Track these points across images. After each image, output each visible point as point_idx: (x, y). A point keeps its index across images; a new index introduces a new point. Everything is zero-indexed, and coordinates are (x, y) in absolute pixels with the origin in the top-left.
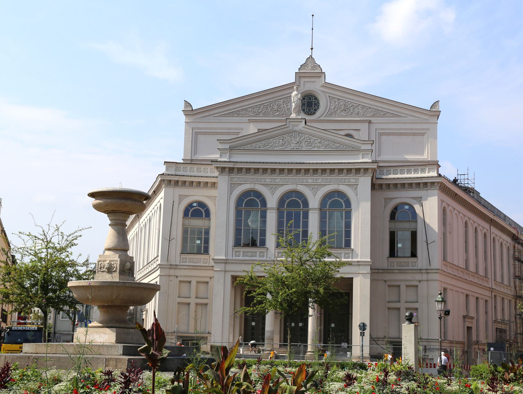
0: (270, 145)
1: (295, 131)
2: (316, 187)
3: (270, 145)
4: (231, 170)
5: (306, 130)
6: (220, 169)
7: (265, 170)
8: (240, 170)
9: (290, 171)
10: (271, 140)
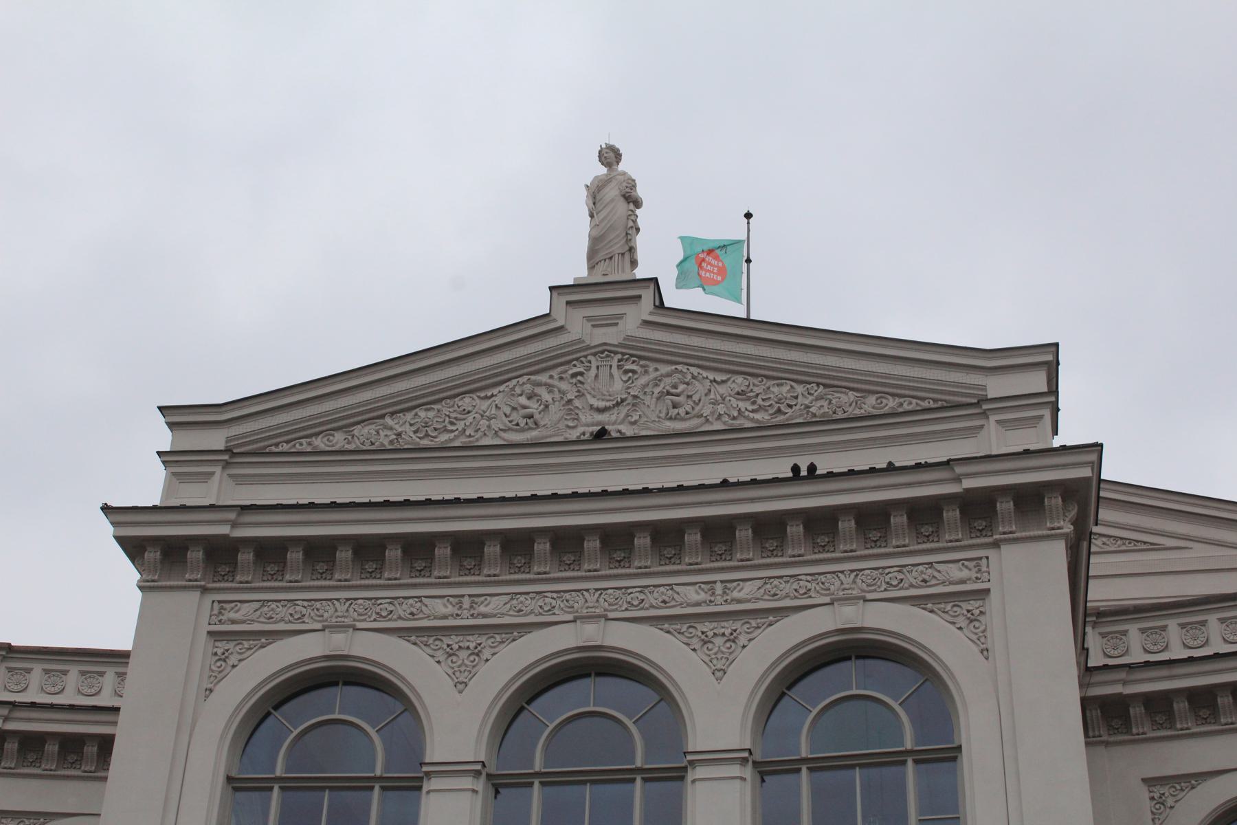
0: (460, 425)
1: (605, 351)
2: (728, 626)
3: (460, 425)
4: (221, 556)
5: (658, 335)
6: (152, 555)
7: (418, 550)
8: (271, 553)
9: (567, 543)
10: (466, 402)
